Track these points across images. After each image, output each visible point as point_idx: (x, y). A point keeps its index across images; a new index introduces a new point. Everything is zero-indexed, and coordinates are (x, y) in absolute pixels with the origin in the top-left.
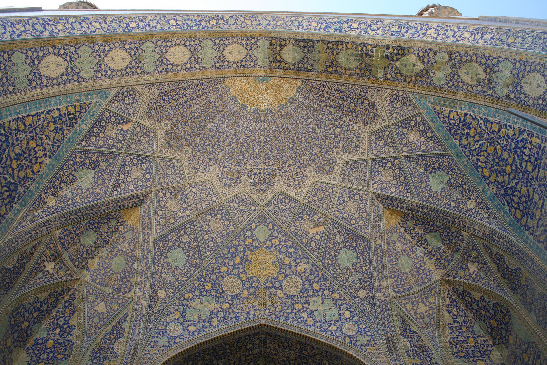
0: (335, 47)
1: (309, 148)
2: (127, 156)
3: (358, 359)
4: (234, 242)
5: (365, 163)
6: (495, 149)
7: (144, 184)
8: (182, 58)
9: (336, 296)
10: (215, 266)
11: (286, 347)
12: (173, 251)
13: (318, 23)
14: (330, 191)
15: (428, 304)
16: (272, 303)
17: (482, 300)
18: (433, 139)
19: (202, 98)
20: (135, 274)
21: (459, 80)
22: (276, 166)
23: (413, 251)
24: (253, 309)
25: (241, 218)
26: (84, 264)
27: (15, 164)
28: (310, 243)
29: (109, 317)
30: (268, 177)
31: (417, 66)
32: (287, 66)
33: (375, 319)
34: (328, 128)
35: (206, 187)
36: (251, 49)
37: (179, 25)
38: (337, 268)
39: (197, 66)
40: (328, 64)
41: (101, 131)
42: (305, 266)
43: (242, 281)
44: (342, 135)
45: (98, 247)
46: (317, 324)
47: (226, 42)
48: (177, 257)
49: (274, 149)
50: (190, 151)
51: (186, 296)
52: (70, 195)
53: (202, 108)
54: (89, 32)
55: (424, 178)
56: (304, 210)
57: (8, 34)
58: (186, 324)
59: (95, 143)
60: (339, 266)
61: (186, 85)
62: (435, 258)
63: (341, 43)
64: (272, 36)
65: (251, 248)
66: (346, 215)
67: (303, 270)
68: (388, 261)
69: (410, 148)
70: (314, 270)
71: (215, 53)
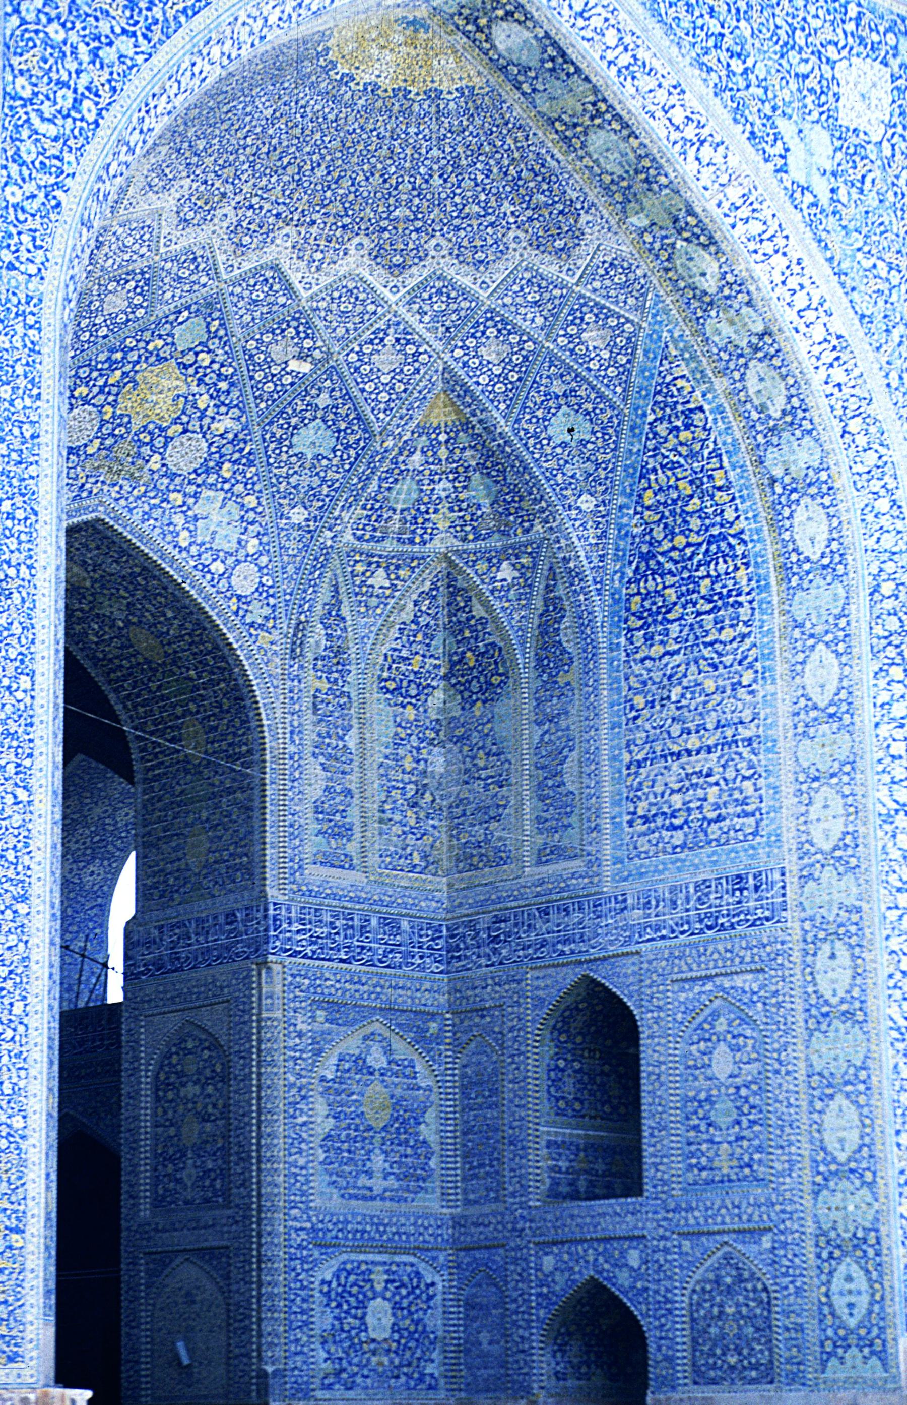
1: (392, 201)
6: (691, 497)
9: (251, 501)
14: (371, 308)
17: (483, 622)
23: (433, 481)
30: (271, 220)
32: (488, 46)
34: (458, 191)
44: (475, 223)
46: (194, 550)
56: (297, 319)
65: (153, 359)
66: (368, 368)
67: (221, 431)
70: (241, 436)
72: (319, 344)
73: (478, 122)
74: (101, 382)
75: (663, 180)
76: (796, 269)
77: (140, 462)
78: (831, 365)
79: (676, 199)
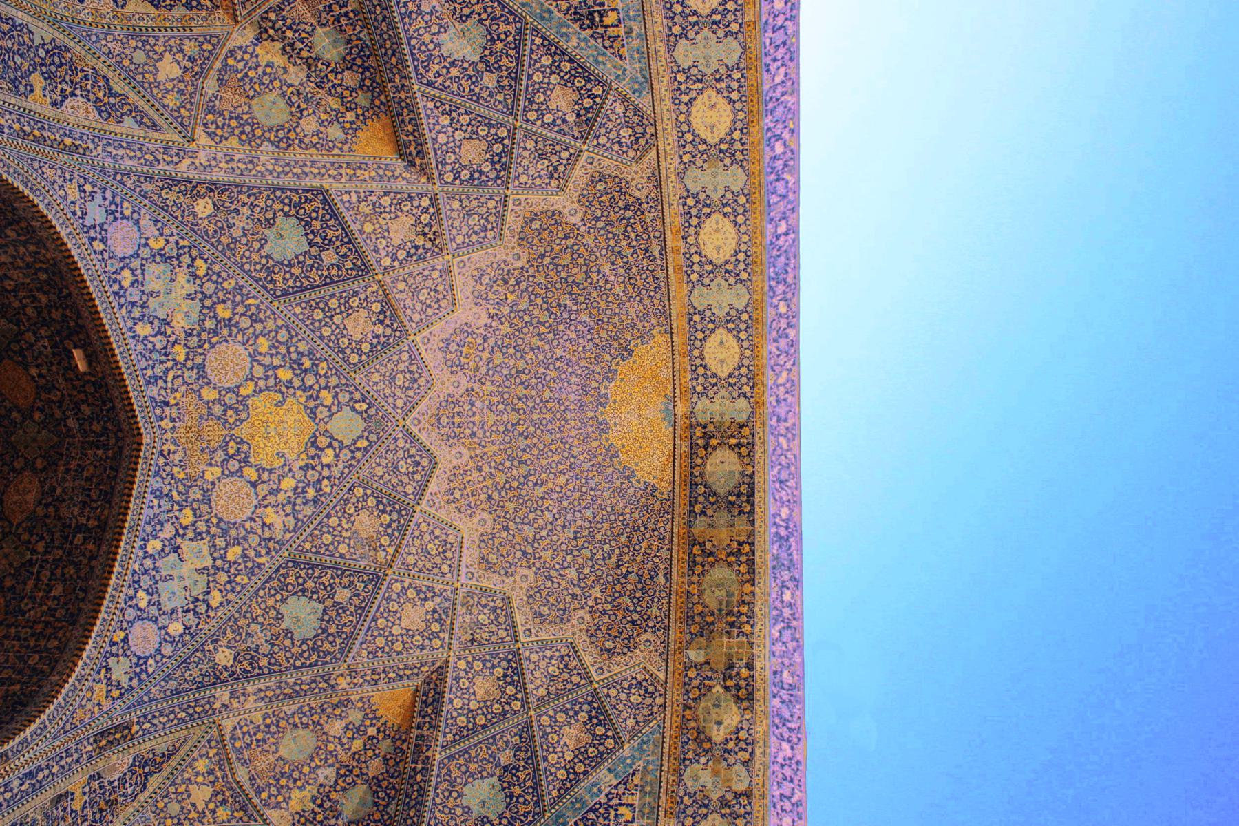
0: (744, 558)
1: (531, 516)
2: (509, 131)
3: (76, 665)
4: (324, 365)
5: (508, 639)
7: (449, 168)
8: (711, 247)
9: (216, 598)
10: (270, 325)
11: (89, 496)
12: (301, 230)
13: (787, 520)
14: (445, 568)
15: (212, 806)
16: (192, 456)
18: (572, 776)
19: (630, 288)
20: (247, 147)
21: (698, 819)
22: (491, 449)
23: (326, 759)
24: (174, 415)
25: (376, 377)
26: (271, 32)
28: (329, 532)
29: (146, 85)
30: (468, 431)
31: (718, 730)
32: (699, 461)
33: (168, 693)
34: (576, 553)
36: (730, 384)
37: (778, 238)
38: (278, 597)
39: (694, 277)
40: (708, 545)
41: (562, 78)
42: (278, 526)
43: (238, 387)
44: (564, 584)
45: (311, 63)
46: (148, 563)
48: (287, 240)
49: (526, 442)
50: (519, 264)
51: (199, 262)
53: (609, 286)
54: (768, 60)
55: (488, 767)
58: (136, 264)
59: (538, 65)
60: (283, 601)
61: (656, 253)
62: (317, 810)
63: (752, 570)
64: (756, 428)
65: (311, 404)
67: (268, 521)
68: (301, 708)
69: (549, 730)
70: (271, 545)
73: (636, 515)
74: (276, 361)
75: (747, 628)
77: (206, 456)
79: (745, 650)
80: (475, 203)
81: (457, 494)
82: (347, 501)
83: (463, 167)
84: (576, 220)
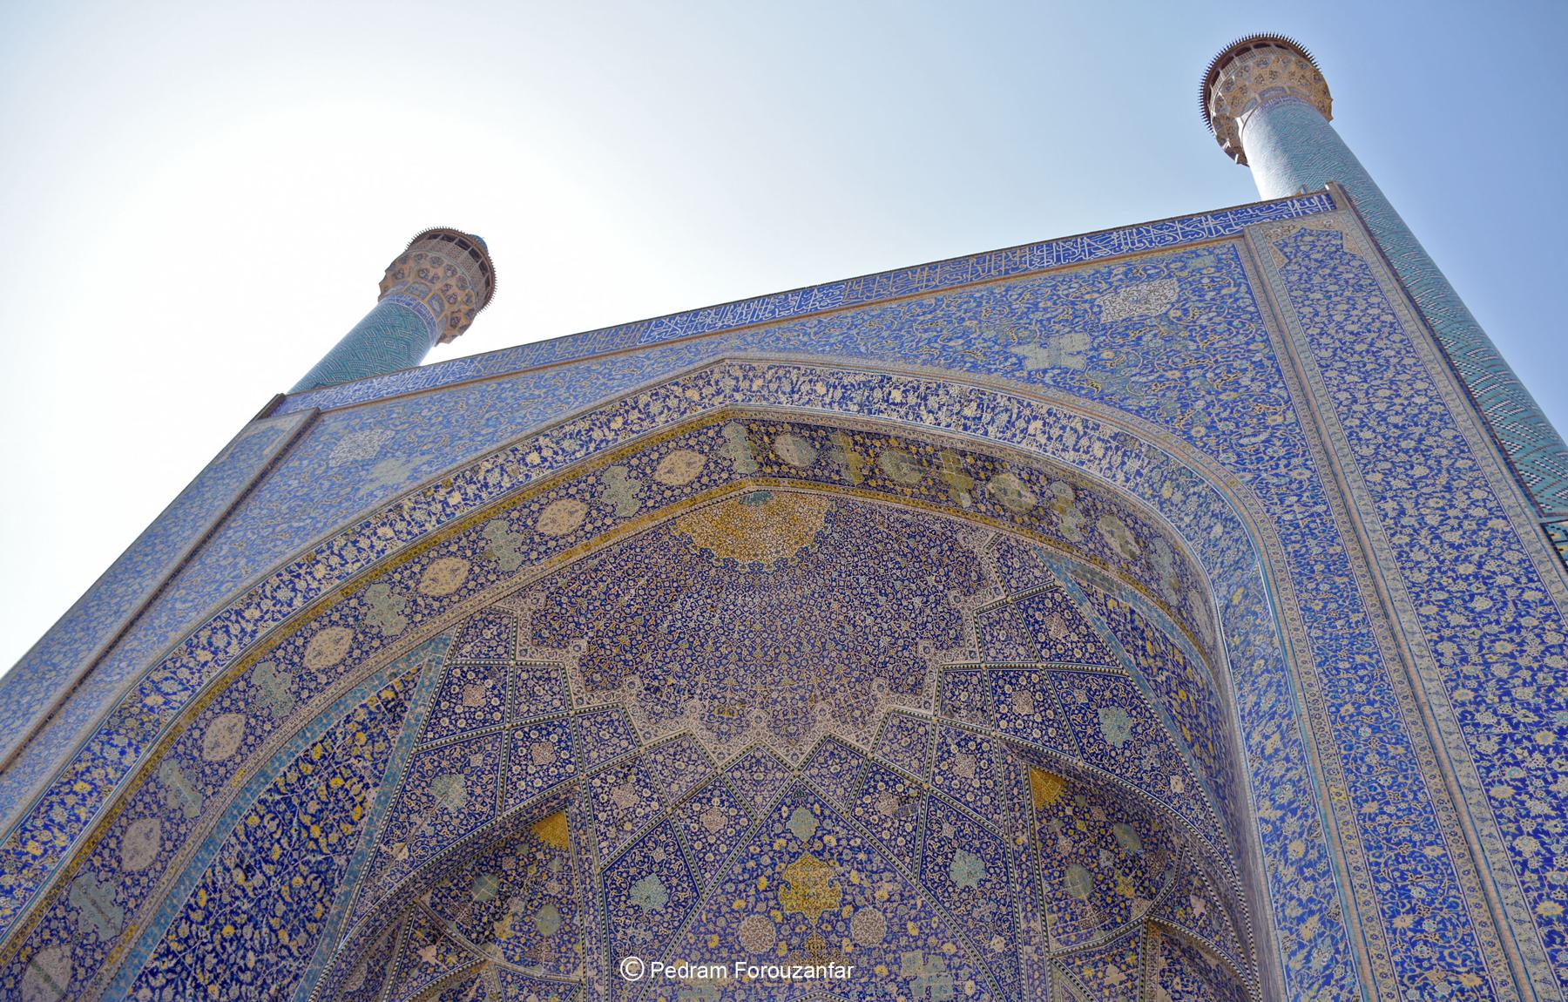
0: (868, 442)
9: (949, 948)
13: (828, 386)
14: (921, 730)
22: (815, 681)
27: (316, 831)
30: (800, 704)
35: (680, 747)
36: (712, 449)
37: (544, 460)
39: (608, 521)
40: (865, 472)
44: (928, 611)
45: (504, 897)
47: (655, 456)
48: (650, 892)
50: (638, 682)
52: (430, 831)
57: (234, 641)
60: (954, 885)
61: (596, 562)
63: (877, 436)
65: (786, 857)
71: (638, 484)
72: (907, 783)
74: (752, 892)
76: (1051, 420)
78: (1123, 463)
80: (589, 739)
81: (857, 713)
82: (868, 822)
83: (558, 758)
84: (584, 643)
